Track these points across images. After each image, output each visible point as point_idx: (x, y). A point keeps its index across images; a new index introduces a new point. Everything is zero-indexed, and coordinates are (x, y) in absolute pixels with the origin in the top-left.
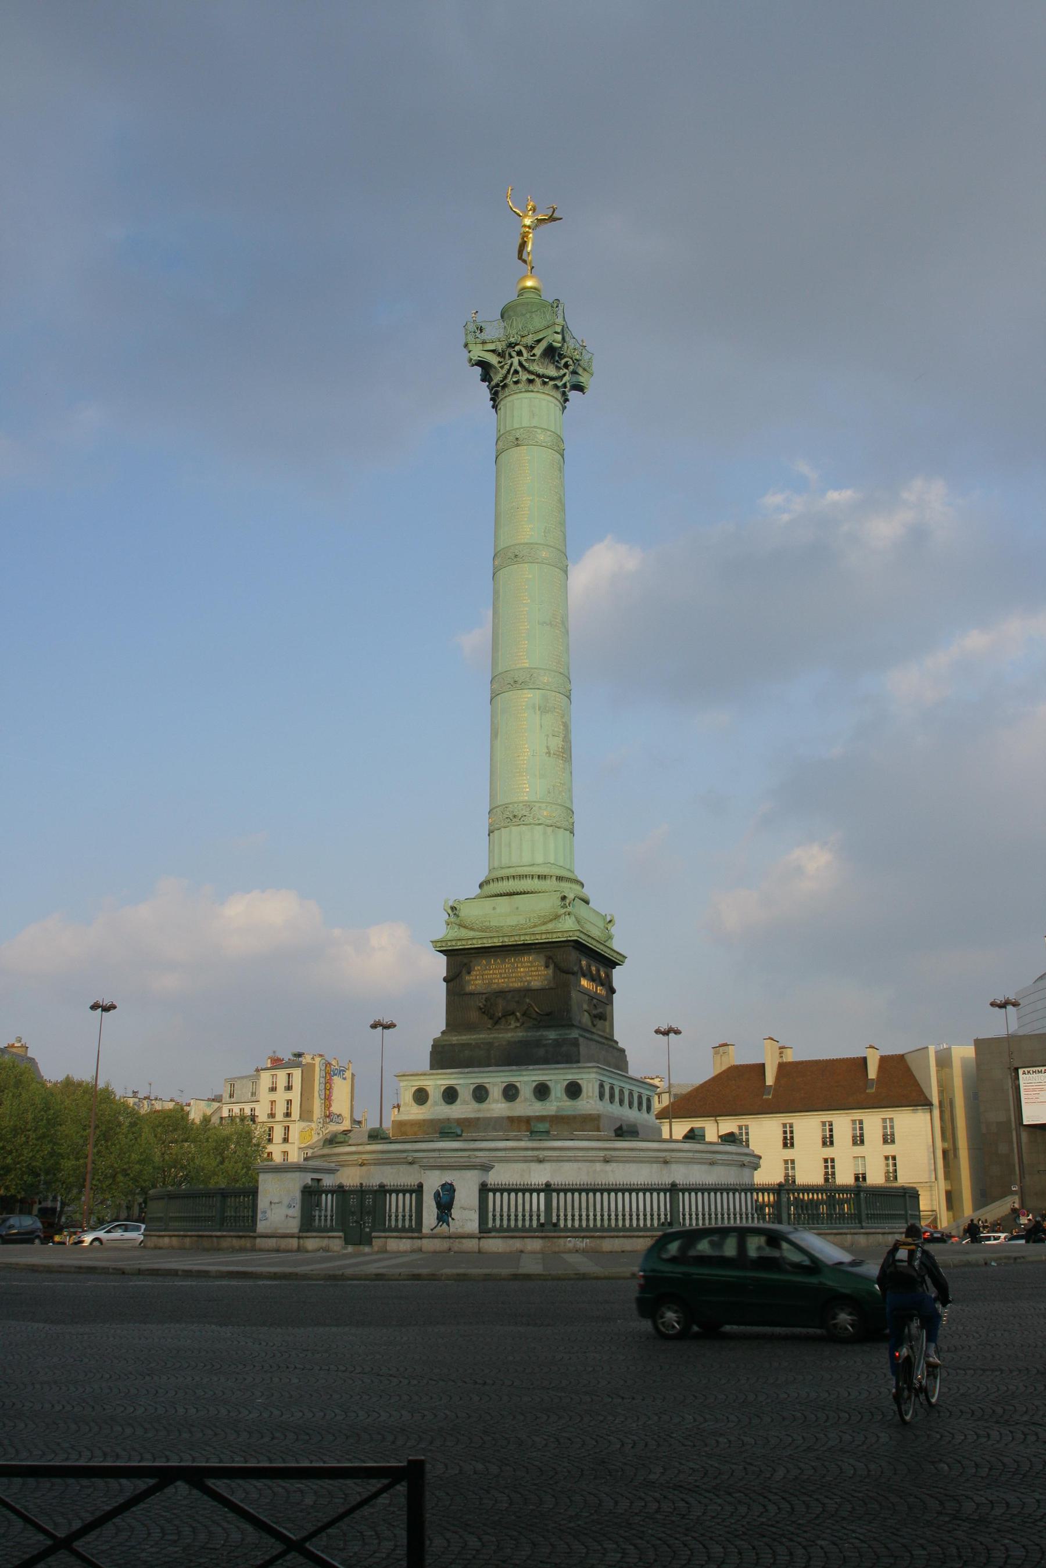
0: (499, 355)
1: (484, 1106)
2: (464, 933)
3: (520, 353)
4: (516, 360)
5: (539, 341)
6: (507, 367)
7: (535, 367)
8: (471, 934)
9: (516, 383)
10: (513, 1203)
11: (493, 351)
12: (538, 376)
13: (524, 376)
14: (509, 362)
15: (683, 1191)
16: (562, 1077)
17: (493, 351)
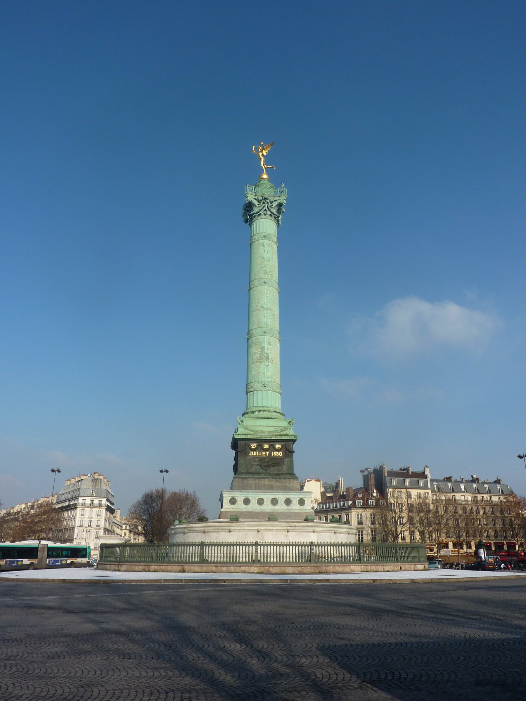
0: (258, 201)
1: (261, 506)
2: (247, 432)
3: (268, 203)
4: (266, 205)
5: (275, 200)
6: (261, 207)
7: (272, 210)
8: (250, 432)
9: (265, 215)
10: (321, 551)
11: (256, 199)
12: (274, 214)
13: (269, 213)
14: (263, 205)
15: (261, 545)
16: (298, 496)
17: (256, 199)
